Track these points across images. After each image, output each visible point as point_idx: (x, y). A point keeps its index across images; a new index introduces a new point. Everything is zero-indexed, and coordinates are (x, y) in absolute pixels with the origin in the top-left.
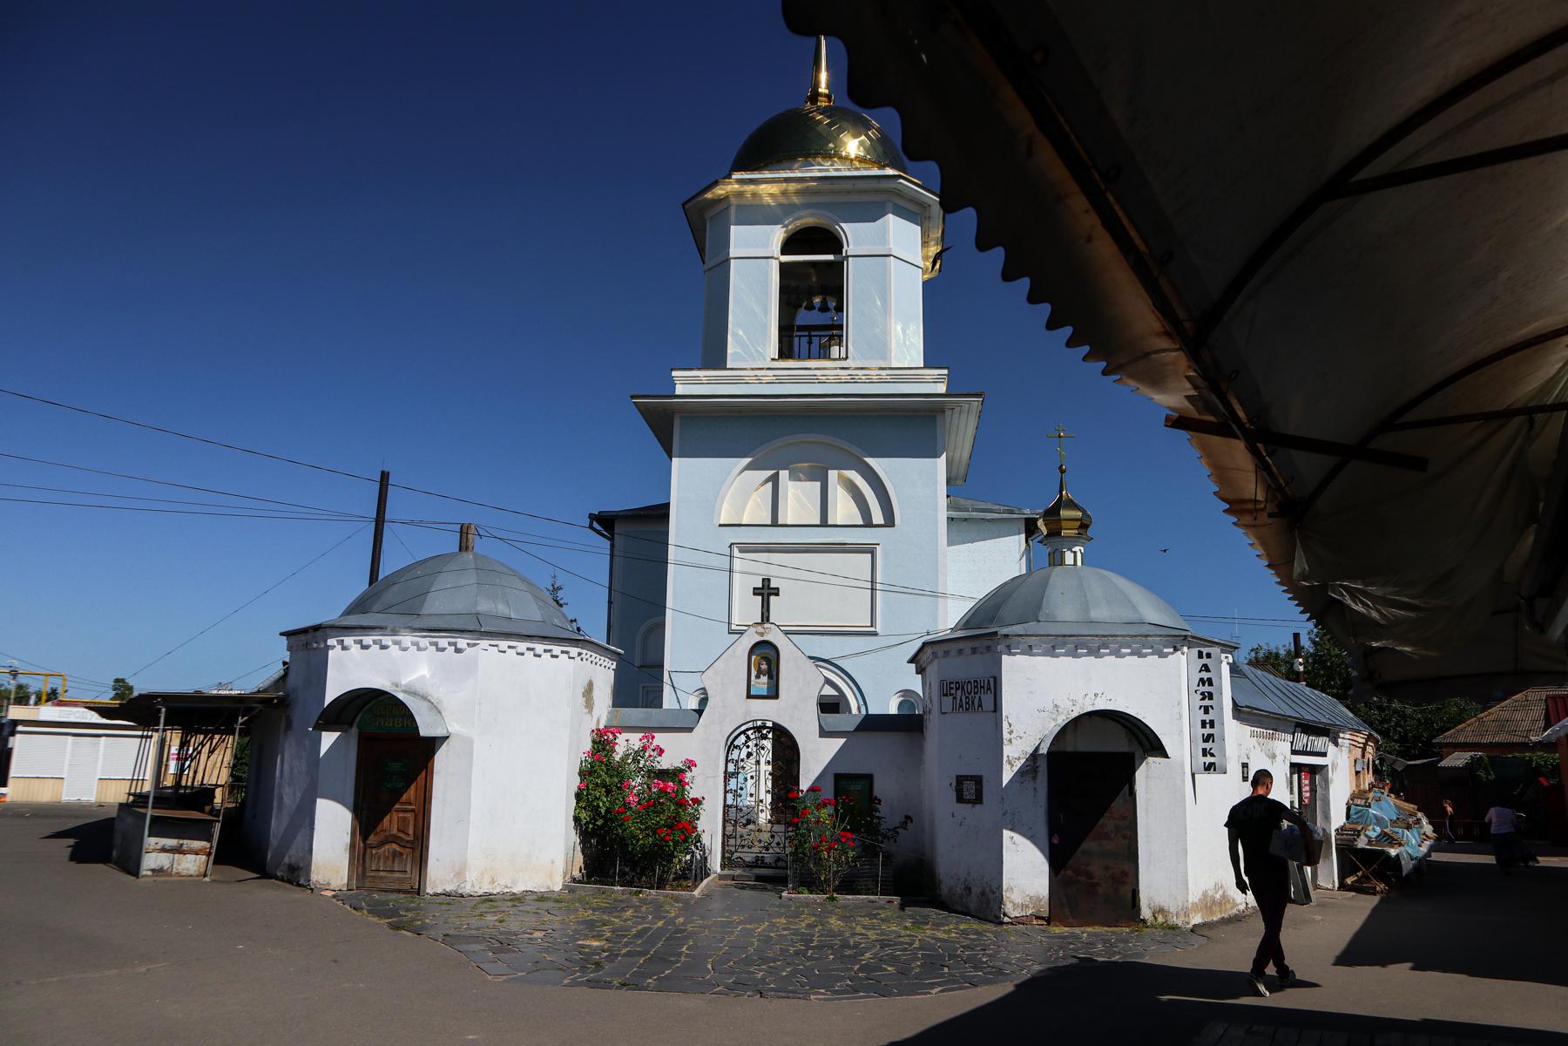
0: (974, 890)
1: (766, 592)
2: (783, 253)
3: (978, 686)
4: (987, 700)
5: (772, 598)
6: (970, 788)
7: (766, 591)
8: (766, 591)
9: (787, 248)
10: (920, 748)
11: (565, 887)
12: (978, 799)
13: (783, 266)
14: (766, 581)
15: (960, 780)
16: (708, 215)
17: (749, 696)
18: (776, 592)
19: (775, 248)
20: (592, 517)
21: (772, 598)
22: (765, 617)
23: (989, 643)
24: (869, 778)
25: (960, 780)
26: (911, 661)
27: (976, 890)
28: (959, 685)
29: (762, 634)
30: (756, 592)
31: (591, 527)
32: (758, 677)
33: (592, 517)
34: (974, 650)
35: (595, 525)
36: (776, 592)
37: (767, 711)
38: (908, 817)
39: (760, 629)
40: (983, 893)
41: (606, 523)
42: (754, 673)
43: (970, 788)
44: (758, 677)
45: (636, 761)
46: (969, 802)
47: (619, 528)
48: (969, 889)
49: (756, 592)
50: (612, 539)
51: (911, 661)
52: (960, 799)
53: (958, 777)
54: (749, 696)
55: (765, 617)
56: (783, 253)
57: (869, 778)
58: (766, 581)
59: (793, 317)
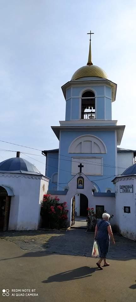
0: (129, 232)
2: (82, 97)
4: (131, 190)
5: (82, 168)
6: (127, 209)
7: (81, 166)
8: (81, 166)
10: (115, 201)
11: (38, 229)
12: (129, 212)
13: (82, 99)
14: (81, 164)
15: (125, 207)
16: (67, 89)
17: (77, 188)
18: (83, 166)
19: (80, 96)
20: (42, 152)
21: (82, 168)
23: (131, 177)
24: (103, 207)
25: (125, 207)
26: (112, 181)
27: (129, 233)
28: (124, 187)
29: (80, 175)
30: (79, 166)
32: (79, 184)
33: (42, 152)
34: (128, 179)
35: (43, 153)
36: (83, 166)
38: (112, 215)
39: (80, 174)
40: (131, 234)
41: (45, 153)
42: (78, 183)
43: (127, 209)
45: (54, 202)
46: (127, 212)
48: (128, 232)
49: (79, 166)
50: (46, 156)
51: (112, 181)
52: (125, 212)
53: (130, 207)
54: (77, 188)
56: (82, 97)
57: (103, 207)
58: (81, 164)
59: (84, 111)
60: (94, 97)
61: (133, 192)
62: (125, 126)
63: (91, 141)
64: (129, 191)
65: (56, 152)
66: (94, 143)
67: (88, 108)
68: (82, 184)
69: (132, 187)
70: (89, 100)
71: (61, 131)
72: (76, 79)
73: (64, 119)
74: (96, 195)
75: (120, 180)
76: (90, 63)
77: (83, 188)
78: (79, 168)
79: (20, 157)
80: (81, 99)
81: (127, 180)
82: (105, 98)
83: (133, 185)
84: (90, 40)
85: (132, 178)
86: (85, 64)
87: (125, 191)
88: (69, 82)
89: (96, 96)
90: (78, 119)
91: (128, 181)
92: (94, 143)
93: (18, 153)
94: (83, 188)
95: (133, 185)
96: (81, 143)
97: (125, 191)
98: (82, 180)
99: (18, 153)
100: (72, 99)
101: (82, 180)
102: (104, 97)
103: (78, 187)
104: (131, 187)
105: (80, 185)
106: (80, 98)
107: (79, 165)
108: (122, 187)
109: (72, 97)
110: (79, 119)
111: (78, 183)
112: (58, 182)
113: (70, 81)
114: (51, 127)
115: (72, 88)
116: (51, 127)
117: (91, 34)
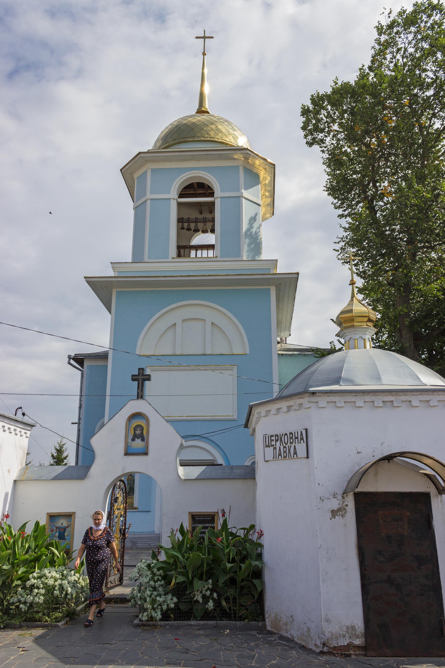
1: (141, 378)
2: (180, 197)
3: (293, 437)
4: (301, 448)
7: (141, 378)
13: (179, 204)
14: (141, 370)
17: (127, 454)
18: (148, 378)
19: (174, 194)
21: (147, 383)
28: (278, 438)
30: (134, 378)
32: (133, 440)
34: (289, 408)
36: (148, 378)
37: (134, 464)
44: (133, 440)
49: (134, 378)
54: (126, 454)
55: (140, 396)
56: (180, 197)
58: (141, 370)
60: (213, 196)
61: (308, 457)
64: (295, 453)
68: (143, 440)
69: (305, 436)
70: (198, 207)
71: (117, 292)
72: (163, 148)
75: (266, 416)
77: (146, 454)
80: (175, 201)
81: (289, 411)
82: (243, 199)
83: (306, 430)
84: (204, 54)
85: (305, 400)
87: (280, 454)
88: (140, 153)
89: (218, 193)
91: (292, 413)
94: (146, 454)
95: (306, 430)
97: (280, 454)
98: (142, 422)
100: (149, 202)
101: (142, 422)
102: (240, 197)
104: (302, 439)
105: (138, 443)
106: (172, 200)
108: (270, 441)
109: (149, 196)
110: (170, 258)
111: (130, 437)
116: (85, 278)
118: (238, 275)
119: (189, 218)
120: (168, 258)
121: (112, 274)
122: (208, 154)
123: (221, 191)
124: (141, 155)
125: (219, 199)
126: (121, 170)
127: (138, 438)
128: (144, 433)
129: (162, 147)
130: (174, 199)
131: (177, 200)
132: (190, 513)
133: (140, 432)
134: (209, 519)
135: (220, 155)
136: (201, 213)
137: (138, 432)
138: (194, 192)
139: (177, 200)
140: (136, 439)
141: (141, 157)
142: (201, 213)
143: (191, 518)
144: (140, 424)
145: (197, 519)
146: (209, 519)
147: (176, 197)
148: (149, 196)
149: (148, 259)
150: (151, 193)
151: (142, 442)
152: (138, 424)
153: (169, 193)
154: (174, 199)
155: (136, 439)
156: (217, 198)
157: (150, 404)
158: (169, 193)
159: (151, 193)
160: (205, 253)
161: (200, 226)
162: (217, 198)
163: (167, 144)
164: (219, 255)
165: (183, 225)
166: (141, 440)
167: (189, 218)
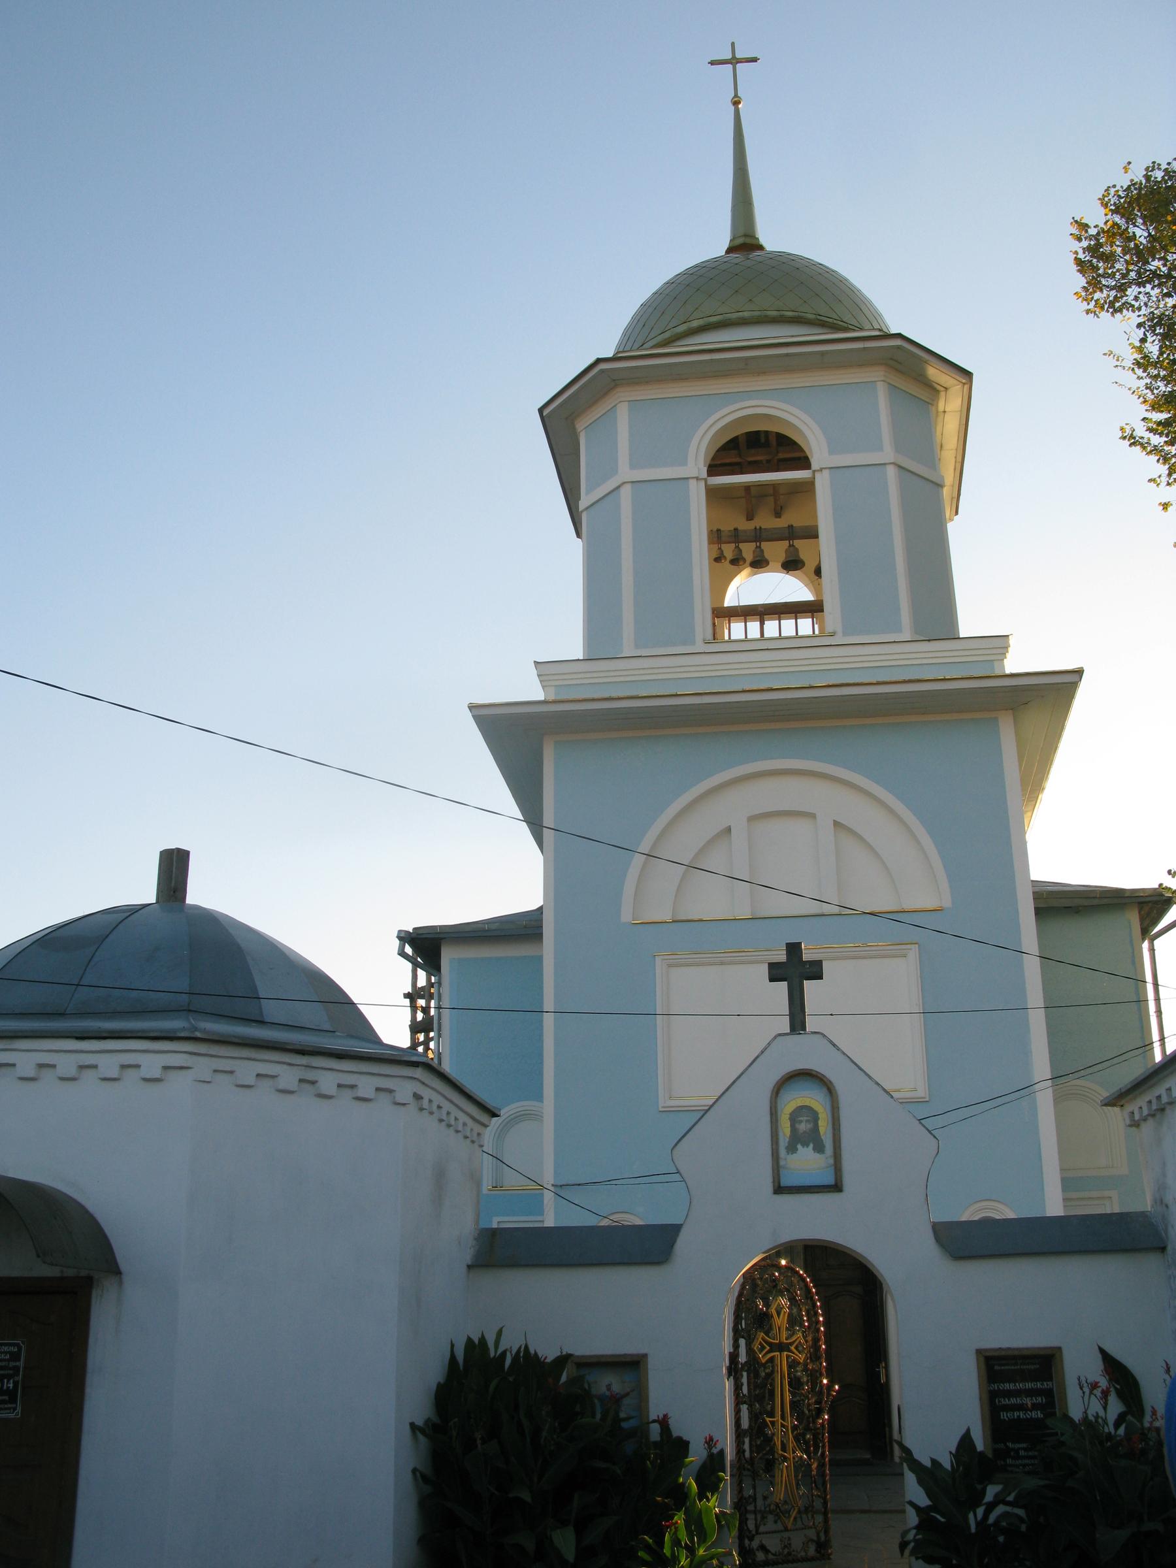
9: (715, 468)
14: (794, 949)
16: (581, 425)
17: (779, 1189)
18: (815, 971)
19: (696, 464)
22: (797, 1021)
31: (402, 953)
32: (792, 1149)
35: (408, 950)
42: (783, 1142)
47: (448, 955)
49: (776, 973)
51: (1118, 1099)
54: (779, 1189)
55: (797, 1021)
58: (794, 949)
62: (1079, 672)
63: (813, 816)
65: (520, 930)
66: (836, 824)
67: (759, 564)
68: (819, 1148)
73: (569, 643)
74: (965, 1242)
76: (745, 243)
77: (836, 1187)
78: (783, 986)
79: (190, 899)
80: (702, 484)
86: (714, 242)
88: (599, 361)
90: (693, 643)
92: (836, 824)
93: (174, 866)
94: (836, 1187)
96: (728, 830)
99: (174, 866)
100: (626, 491)
103: (786, 1181)
106: (693, 483)
107: (781, 957)
109: (625, 472)
111: (783, 1142)
112: (548, 1179)
113: (610, 355)
114: (472, 707)
115: (623, 415)
116: (472, 707)
117: (734, 61)
118: (910, 681)
119: (736, 529)
120: (693, 643)
121: (539, 695)
122: (787, 355)
123: (832, 452)
124: (603, 366)
125: (826, 473)
126: (541, 410)
127: (805, 1144)
128: (822, 1130)
129: (651, 344)
130: (697, 479)
131: (706, 480)
132: (979, 1352)
133: (810, 1126)
134: (1033, 1367)
135: (823, 353)
136: (750, 517)
137: (803, 1127)
138: (737, 460)
139: (706, 480)
140: (799, 1146)
141: (602, 371)
142: (750, 517)
143: (983, 1367)
144: (807, 1102)
145: (997, 1368)
146: (1033, 1367)
147: (704, 474)
148: (625, 472)
149: (637, 646)
150: (633, 466)
151: (818, 1155)
152: (800, 1102)
153: (684, 462)
154: (697, 479)
155: (799, 1146)
156: (821, 470)
157: (834, 1045)
158: (684, 462)
159: (633, 466)
160: (788, 626)
161: (748, 550)
162: (821, 470)
163: (667, 335)
164: (839, 629)
165: (737, 547)
166: (814, 1149)
167: (736, 529)
